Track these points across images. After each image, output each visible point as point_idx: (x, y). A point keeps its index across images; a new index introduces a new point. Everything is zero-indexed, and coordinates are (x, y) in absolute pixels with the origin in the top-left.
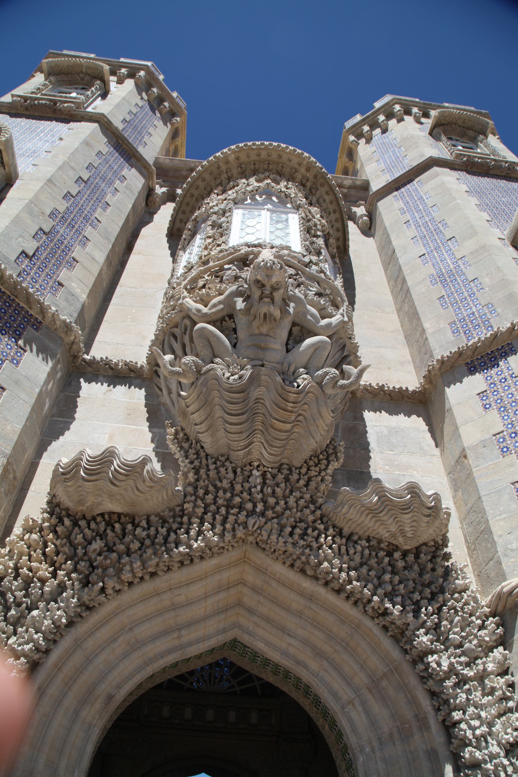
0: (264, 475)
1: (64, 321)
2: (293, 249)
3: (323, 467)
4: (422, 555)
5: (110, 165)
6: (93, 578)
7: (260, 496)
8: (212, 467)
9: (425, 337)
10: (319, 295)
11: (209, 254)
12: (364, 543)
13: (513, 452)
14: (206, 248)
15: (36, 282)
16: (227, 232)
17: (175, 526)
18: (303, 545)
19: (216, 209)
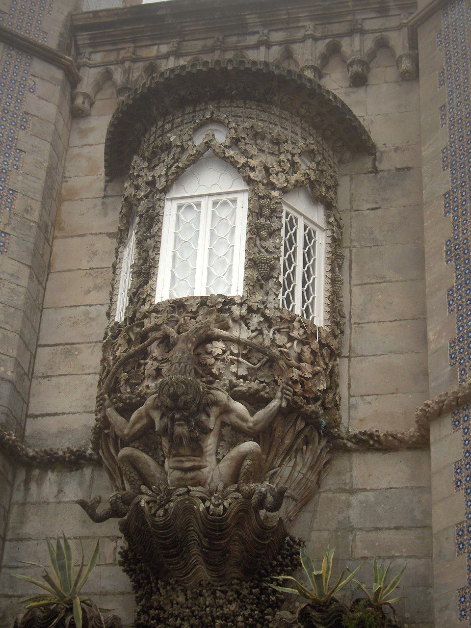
13: (466, 550)
14: (131, 301)
16: (152, 271)
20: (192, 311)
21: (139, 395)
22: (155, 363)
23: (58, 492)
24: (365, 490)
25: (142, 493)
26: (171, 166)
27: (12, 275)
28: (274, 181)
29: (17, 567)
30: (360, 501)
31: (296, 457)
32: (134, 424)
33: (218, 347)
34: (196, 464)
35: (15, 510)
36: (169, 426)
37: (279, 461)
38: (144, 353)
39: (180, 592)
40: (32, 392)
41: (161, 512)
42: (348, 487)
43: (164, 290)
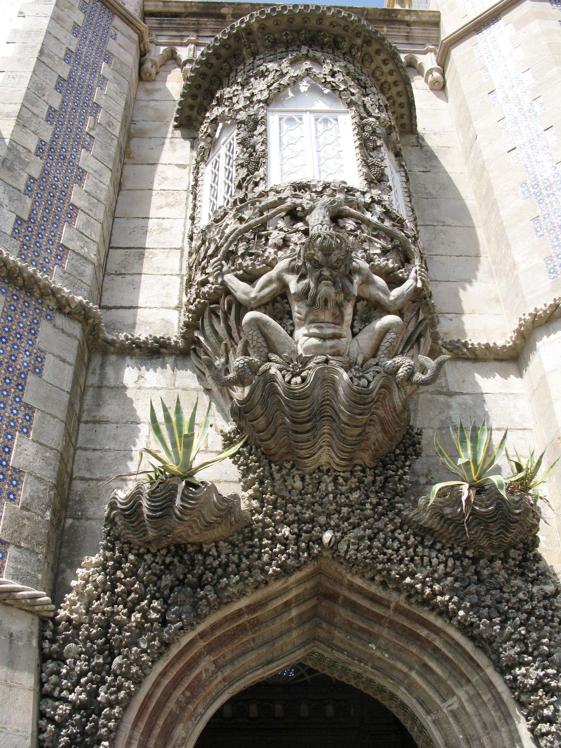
0: (335, 480)
1: (81, 302)
2: (350, 184)
3: (400, 464)
4: (510, 561)
5: (91, 41)
6: (171, 616)
7: (334, 506)
8: (277, 476)
9: (515, 272)
10: (385, 252)
11: (246, 195)
12: (447, 552)
14: (239, 187)
15: (38, 256)
17: (247, 550)
18: (383, 560)
19: (242, 116)
20: (316, 192)
21: (264, 262)
22: (281, 233)
23: (138, 378)
24: (462, 394)
25: (269, 360)
26: (272, 84)
27: (95, 171)
28: (370, 110)
29: (95, 450)
30: (458, 403)
31: (412, 347)
32: (263, 288)
33: (350, 224)
34: (337, 331)
35: (90, 393)
36: (312, 285)
37: (401, 349)
38: (264, 225)
39: (297, 476)
40: (105, 286)
41: (298, 379)
42: (445, 390)
43: (279, 173)
